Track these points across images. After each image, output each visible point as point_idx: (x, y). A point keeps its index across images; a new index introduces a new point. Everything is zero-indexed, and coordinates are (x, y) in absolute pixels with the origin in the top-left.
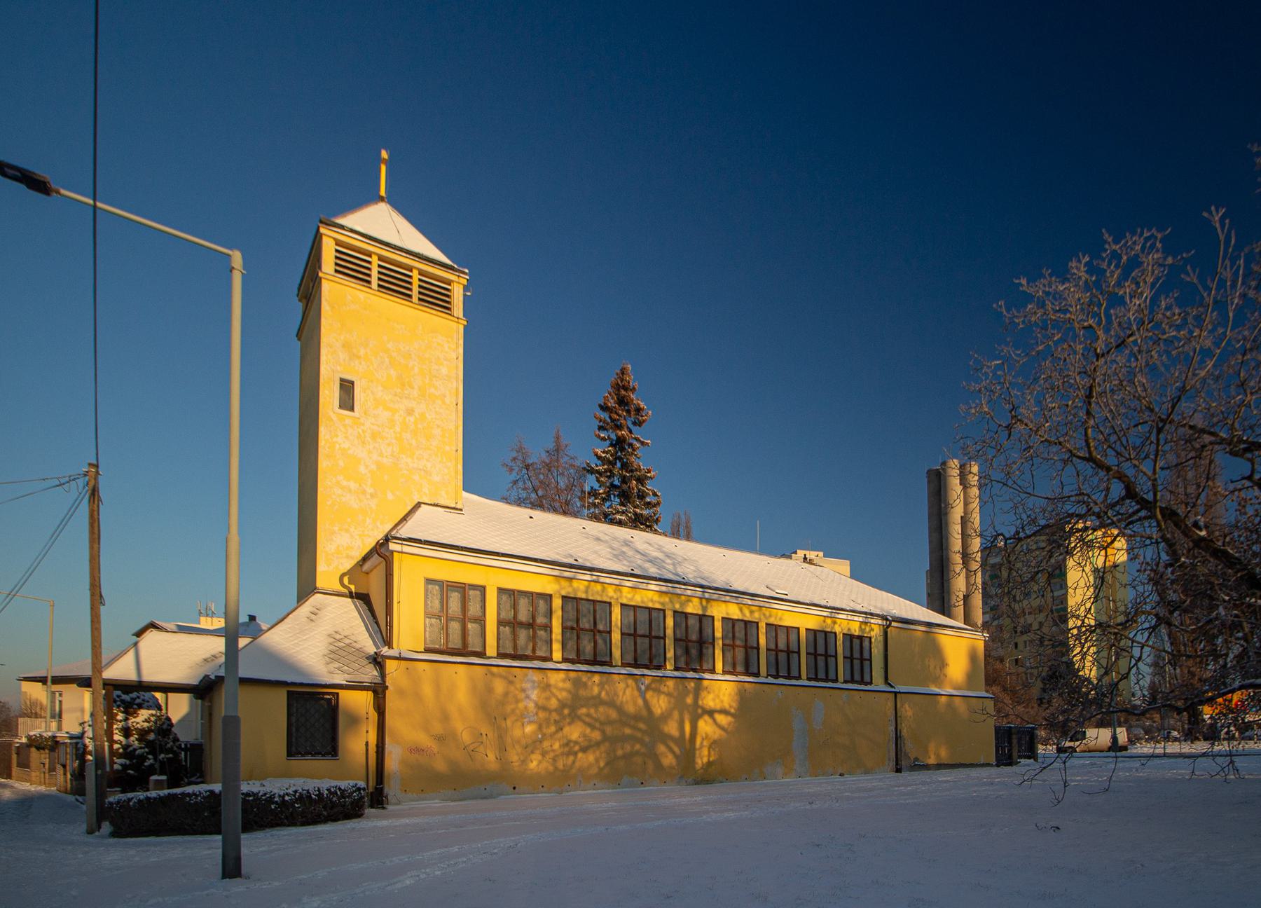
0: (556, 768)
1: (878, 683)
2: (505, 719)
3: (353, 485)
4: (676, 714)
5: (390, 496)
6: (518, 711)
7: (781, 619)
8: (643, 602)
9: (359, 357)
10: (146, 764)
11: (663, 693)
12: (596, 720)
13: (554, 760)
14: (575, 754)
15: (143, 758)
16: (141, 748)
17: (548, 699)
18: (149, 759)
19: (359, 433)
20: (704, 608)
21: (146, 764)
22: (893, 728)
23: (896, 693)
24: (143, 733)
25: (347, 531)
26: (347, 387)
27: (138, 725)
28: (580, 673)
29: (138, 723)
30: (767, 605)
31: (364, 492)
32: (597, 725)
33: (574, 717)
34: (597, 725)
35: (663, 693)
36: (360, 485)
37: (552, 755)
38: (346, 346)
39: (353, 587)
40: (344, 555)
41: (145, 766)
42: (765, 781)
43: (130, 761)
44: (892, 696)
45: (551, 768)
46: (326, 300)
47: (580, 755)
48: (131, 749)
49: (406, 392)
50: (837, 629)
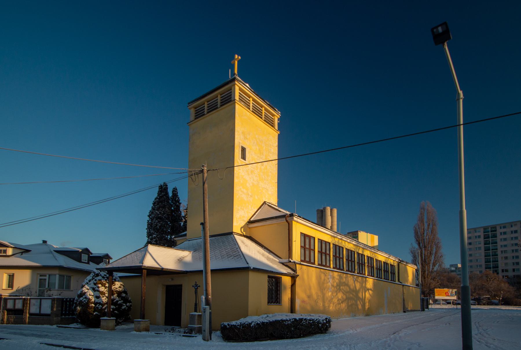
0: (336, 309)
1: (397, 282)
2: (324, 290)
3: (245, 191)
4: (361, 289)
5: (256, 198)
6: (327, 287)
7: (378, 257)
8: (350, 248)
9: (247, 139)
10: (123, 308)
11: (359, 282)
12: (345, 291)
13: (336, 306)
14: (340, 304)
15: (121, 305)
16: (120, 300)
17: (334, 282)
18: (124, 306)
19: (247, 170)
20: (363, 252)
21: (123, 308)
22: (403, 297)
23: (403, 285)
24: (119, 293)
25: (243, 210)
26: (243, 150)
27: (117, 289)
28: (341, 273)
29: (116, 289)
30: (377, 252)
31: (248, 194)
32: (345, 293)
33: (340, 290)
34: (345, 293)
35: (359, 282)
36: (247, 192)
37: (335, 304)
38: (243, 133)
39: (244, 233)
40: (242, 219)
41: (122, 309)
42: (380, 315)
43: (115, 306)
44: (402, 286)
45: (335, 309)
46: (237, 112)
47: (341, 304)
48: (115, 301)
49: (261, 156)
50: (389, 262)
